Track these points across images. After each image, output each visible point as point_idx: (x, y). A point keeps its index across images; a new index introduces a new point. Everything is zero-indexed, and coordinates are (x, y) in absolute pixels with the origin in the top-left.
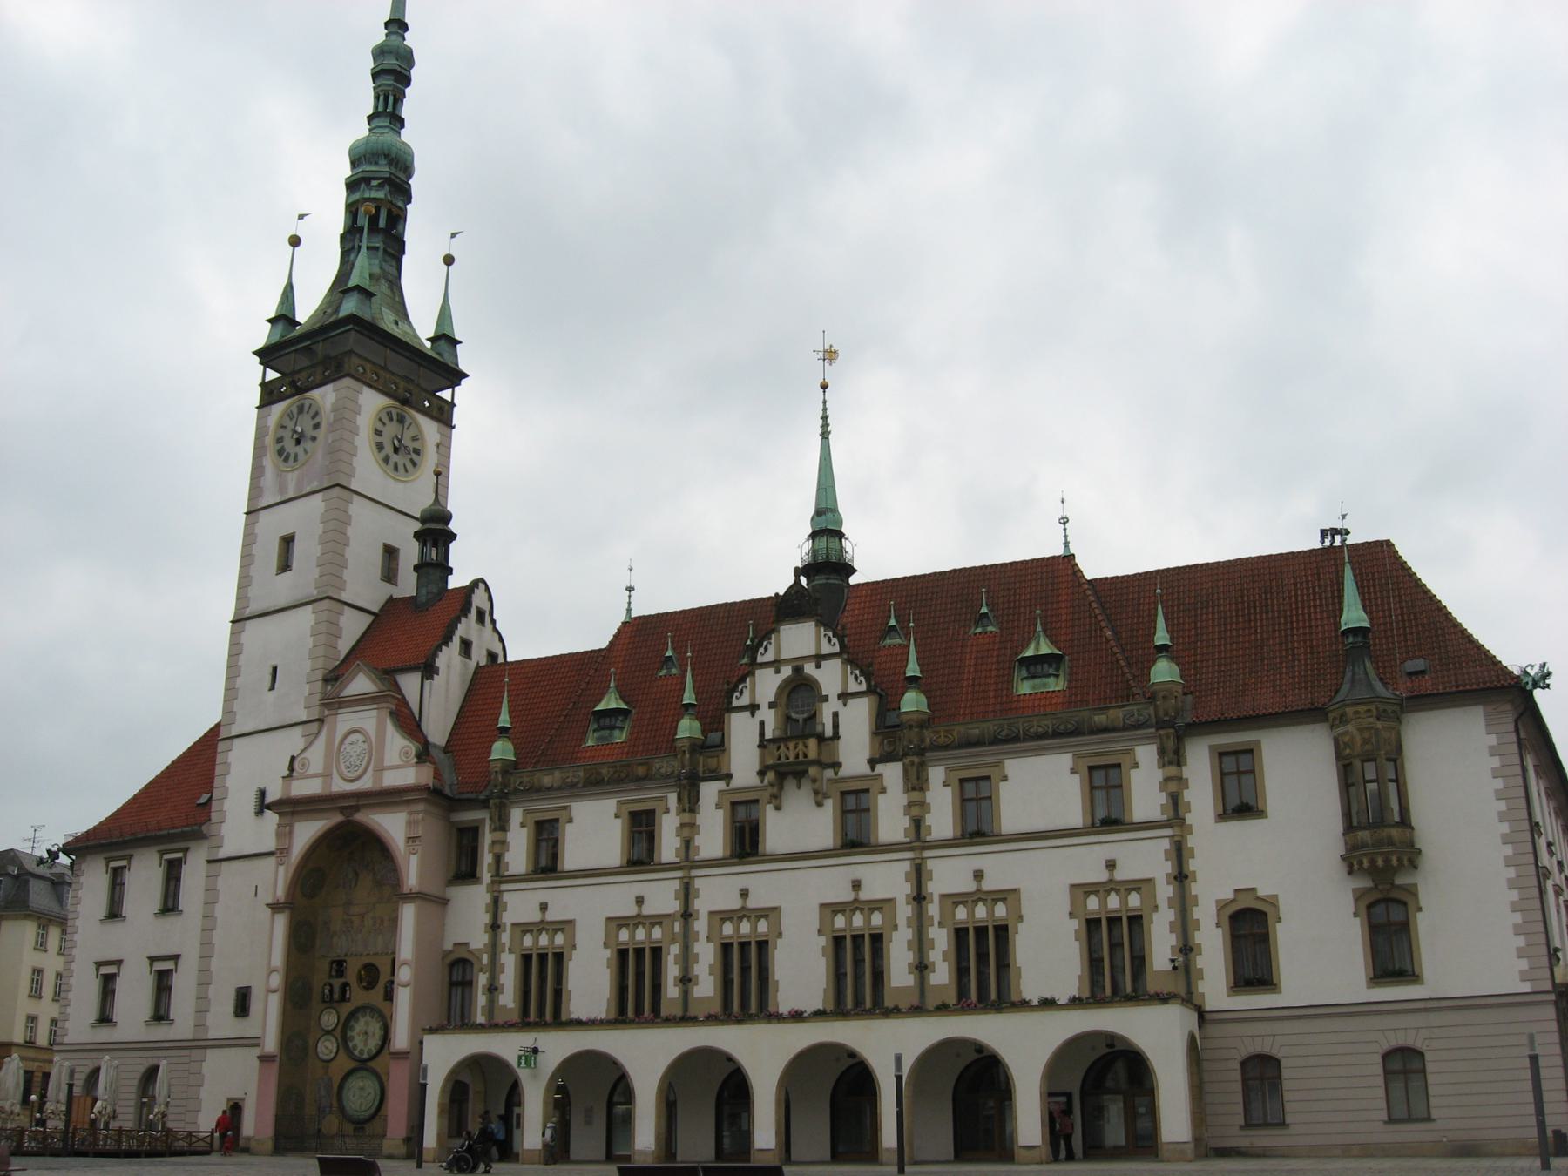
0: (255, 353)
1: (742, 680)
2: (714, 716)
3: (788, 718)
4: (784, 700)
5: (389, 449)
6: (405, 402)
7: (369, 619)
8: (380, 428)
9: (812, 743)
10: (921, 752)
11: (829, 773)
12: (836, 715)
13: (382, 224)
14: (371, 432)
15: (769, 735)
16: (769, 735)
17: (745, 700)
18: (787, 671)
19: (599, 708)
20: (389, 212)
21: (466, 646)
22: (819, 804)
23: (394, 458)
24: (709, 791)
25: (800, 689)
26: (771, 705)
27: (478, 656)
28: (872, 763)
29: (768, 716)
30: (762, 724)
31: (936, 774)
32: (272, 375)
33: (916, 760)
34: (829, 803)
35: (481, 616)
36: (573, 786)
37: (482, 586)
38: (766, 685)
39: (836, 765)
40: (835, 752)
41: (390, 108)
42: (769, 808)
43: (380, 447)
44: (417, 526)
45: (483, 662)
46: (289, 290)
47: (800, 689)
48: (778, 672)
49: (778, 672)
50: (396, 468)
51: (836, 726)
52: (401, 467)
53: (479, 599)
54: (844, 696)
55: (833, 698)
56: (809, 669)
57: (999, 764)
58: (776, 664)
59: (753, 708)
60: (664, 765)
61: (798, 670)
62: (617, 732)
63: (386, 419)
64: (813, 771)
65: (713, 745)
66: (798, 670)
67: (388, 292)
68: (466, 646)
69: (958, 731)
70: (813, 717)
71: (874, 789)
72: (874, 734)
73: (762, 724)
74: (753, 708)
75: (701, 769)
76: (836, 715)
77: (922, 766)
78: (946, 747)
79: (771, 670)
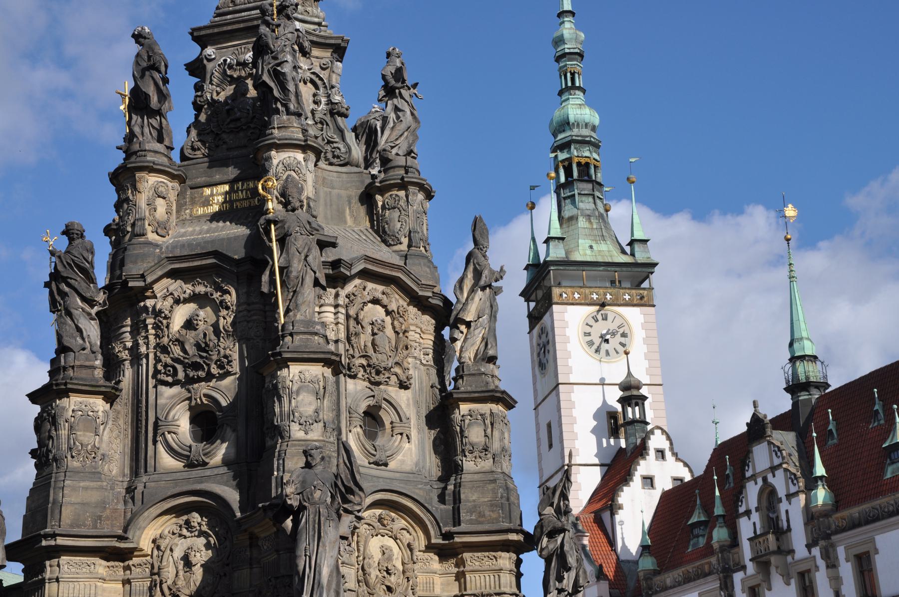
0: (521, 295)
1: (741, 493)
2: (731, 521)
3: (768, 516)
4: (765, 504)
5: (597, 341)
6: (603, 305)
7: (606, 468)
8: (588, 329)
9: (771, 537)
10: (827, 537)
11: (789, 558)
12: (787, 512)
13: (575, 174)
14: (581, 335)
15: (758, 533)
16: (758, 533)
17: (742, 510)
18: (760, 481)
19: (690, 522)
20: (579, 164)
21: (649, 481)
22: (788, 584)
23: (605, 346)
24: (738, 577)
25: (769, 496)
26: (757, 509)
27: (664, 484)
28: (809, 547)
29: (755, 517)
30: (754, 524)
31: (841, 551)
32: (532, 305)
33: (822, 543)
34: (793, 581)
35: (661, 453)
36: (679, 584)
37: (658, 432)
38: (752, 492)
39: (792, 552)
40: (789, 541)
41: (569, 84)
42: (766, 591)
43: (591, 343)
44: (620, 394)
45: (669, 486)
46: (533, 239)
47: (769, 496)
48: (756, 483)
49: (756, 483)
50: (608, 353)
51: (788, 521)
52: (612, 352)
53: (657, 441)
54: (789, 496)
55: (784, 499)
56: (770, 477)
57: (873, 541)
58: (754, 477)
59: (748, 513)
60: (713, 560)
61: (765, 479)
62: (701, 539)
63: (592, 322)
64: (773, 559)
65: (734, 541)
66: (765, 479)
67: (587, 225)
68: (649, 481)
69: (855, 511)
70: (777, 517)
71: (813, 569)
72: (806, 524)
73: (754, 524)
74: (748, 513)
75: (732, 563)
76: (787, 512)
77: (833, 546)
78: (844, 530)
79: (753, 482)
